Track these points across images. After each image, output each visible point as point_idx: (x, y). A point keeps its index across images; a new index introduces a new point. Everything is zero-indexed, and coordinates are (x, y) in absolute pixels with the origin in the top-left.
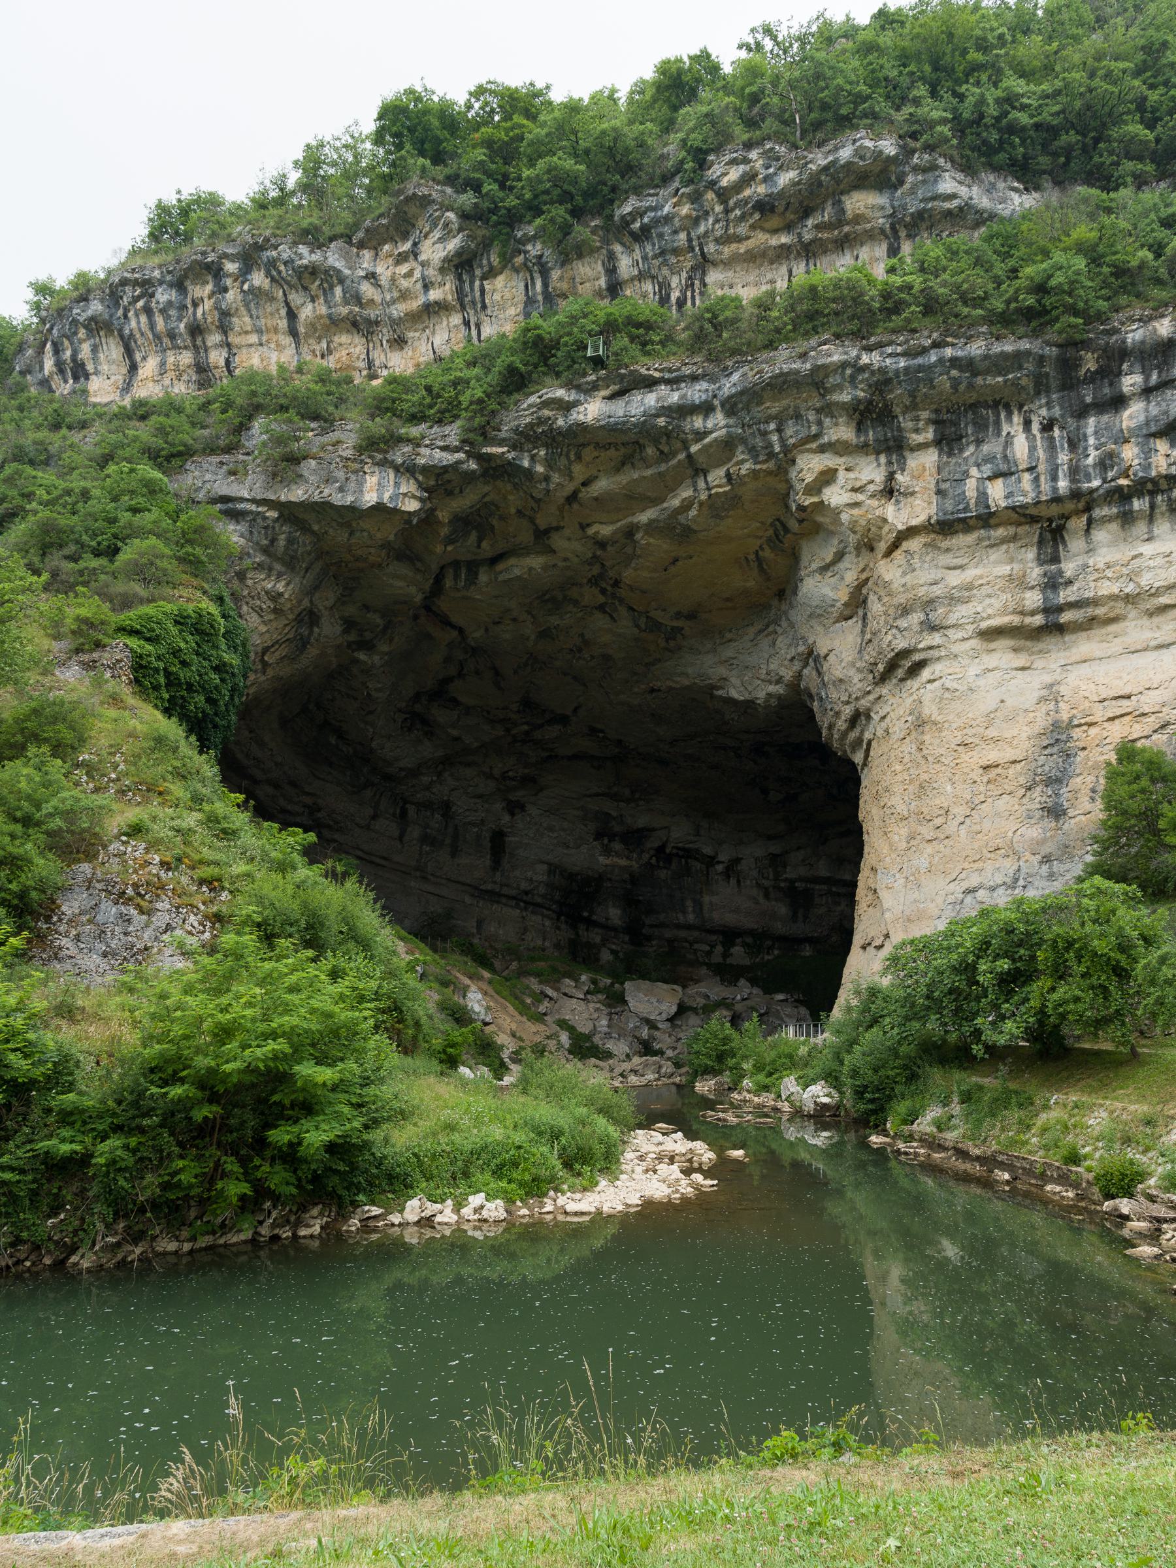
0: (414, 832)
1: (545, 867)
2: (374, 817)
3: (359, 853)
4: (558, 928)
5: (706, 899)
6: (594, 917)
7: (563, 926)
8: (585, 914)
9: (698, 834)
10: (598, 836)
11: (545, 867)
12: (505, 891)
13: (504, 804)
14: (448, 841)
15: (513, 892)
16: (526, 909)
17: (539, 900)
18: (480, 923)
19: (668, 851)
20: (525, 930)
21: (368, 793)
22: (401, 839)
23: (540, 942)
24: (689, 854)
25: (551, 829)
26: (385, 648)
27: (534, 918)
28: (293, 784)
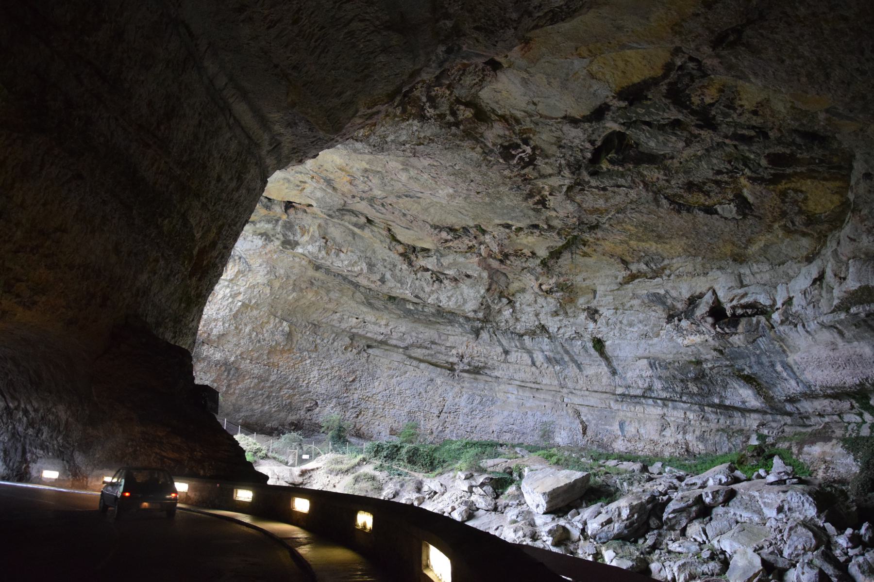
0: (539, 358)
1: (645, 361)
2: (506, 352)
3: (518, 383)
4: (707, 420)
5: (791, 359)
6: (727, 403)
7: (712, 417)
8: (717, 401)
9: (742, 285)
10: (670, 318)
11: (645, 361)
12: (633, 392)
13: (586, 313)
14: (567, 358)
15: (639, 392)
16: (665, 405)
17: (664, 395)
18: (622, 425)
19: (728, 313)
20: (663, 429)
21: (484, 335)
22: (534, 364)
23: (680, 437)
24: (756, 309)
25: (631, 325)
26: (306, 238)
27: (675, 413)
28: (433, 343)
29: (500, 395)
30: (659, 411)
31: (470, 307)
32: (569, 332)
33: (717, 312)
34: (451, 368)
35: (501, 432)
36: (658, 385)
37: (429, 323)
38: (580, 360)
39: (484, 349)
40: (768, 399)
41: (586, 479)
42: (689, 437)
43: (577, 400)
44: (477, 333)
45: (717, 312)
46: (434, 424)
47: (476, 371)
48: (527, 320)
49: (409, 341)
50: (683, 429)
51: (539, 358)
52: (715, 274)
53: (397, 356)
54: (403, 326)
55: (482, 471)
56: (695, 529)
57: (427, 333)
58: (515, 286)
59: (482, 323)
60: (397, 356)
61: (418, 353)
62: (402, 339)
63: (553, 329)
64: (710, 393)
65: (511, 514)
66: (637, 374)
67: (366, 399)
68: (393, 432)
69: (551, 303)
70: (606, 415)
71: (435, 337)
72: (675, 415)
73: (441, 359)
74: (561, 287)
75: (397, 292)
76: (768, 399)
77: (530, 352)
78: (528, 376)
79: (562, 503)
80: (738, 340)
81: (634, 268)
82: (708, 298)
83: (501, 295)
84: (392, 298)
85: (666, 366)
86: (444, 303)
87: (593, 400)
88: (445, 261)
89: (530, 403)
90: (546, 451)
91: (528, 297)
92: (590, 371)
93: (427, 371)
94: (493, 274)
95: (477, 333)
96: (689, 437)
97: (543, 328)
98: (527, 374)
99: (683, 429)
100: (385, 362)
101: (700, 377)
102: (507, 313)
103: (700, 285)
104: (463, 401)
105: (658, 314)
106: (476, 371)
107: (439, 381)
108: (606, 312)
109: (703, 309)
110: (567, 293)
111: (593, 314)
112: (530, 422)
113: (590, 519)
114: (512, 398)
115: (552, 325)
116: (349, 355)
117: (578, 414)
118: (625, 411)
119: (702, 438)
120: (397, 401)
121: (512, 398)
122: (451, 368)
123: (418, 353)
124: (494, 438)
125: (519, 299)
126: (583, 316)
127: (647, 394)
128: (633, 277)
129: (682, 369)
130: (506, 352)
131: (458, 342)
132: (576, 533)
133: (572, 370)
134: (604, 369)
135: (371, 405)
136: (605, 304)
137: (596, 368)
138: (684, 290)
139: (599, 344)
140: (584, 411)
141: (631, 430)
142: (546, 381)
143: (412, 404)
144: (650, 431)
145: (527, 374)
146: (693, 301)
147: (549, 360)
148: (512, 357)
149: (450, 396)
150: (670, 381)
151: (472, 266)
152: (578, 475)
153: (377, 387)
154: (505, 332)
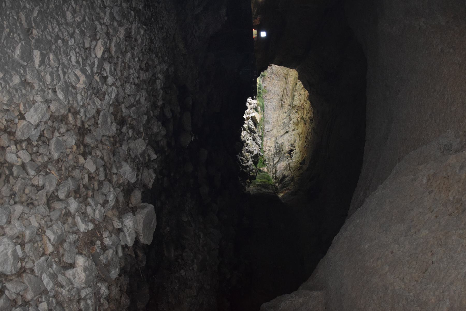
2: (286, 113)
21: (289, 107)
29: (276, 112)
30: (273, 146)
31: (295, 103)
32: (290, 126)
33: (292, 151)
34: (282, 100)
35: (267, 113)
36: (278, 145)
37: (292, 93)
38: (284, 129)
39: (286, 107)
40: (275, 164)
41: (258, 123)
42: (268, 152)
43: (275, 130)
44: (290, 105)
45: (292, 151)
46: (268, 97)
47: (282, 106)
48: (292, 116)
49: (287, 89)
50: (269, 150)
51: (284, 120)
52: (298, 149)
53: (284, 86)
54: (291, 87)
55: (258, 106)
56: (251, 138)
57: (290, 93)
58: (299, 112)
59: (292, 106)
60: (284, 86)
61: (285, 91)
62: (288, 87)
63: (291, 122)
64: (277, 154)
65: (251, 111)
66: (281, 140)
67: (273, 79)
68: (265, 87)
69: (296, 121)
70: (272, 136)
71: (289, 95)
72: (272, 149)
73: (284, 97)
74: (298, 122)
75: (297, 85)
76: (275, 164)
77: (286, 118)
78: (280, 118)
79: (254, 119)
80: (286, 155)
81: (301, 135)
82: (294, 149)
83: (297, 110)
84: (296, 84)
85: (282, 145)
86: (296, 97)
87: (275, 133)
88: (303, 96)
89: (274, 119)
90: (263, 119)
91: (297, 116)
92: (282, 132)
93: (281, 94)
94: (301, 107)
95: (290, 105)
96: (268, 152)
97: (291, 120)
98: (281, 118)
99: (269, 150)
100: (283, 83)
101: (280, 151)
102: (294, 112)
103: (297, 147)
104: (274, 104)
105: (293, 142)
106: (282, 106)
107: (279, 97)
108: (294, 132)
109: (292, 148)
110: (297, 124)
111: (294, 130)
112: (270, 120)
113: (251, 123)
114: (275, 115)
115: (291, 122)
116: (283, 74)
117: (272, 130)
118: (273, 140)
119: (267, 154)
120: (273, 87)
121: (275, 115)
122: (282, 100)
123: (285, 91)
124: (265, 111)
125: (297, 114)
126: (293, 128)
127: (277, 143)
128: (299, 136)
129: (281, 148)
130: (286, 113)
131: (288, 101)
132: (249, 121)
133: (282, 128)
134: (282, 134)
135: (271, 80)
136: (296, 131)
137: (282, 132)
138: (296, 145)
139: (287, 132)
140: (273, 131)
141: (269, 141)
142: (279, 122)
143: (272, 91)
144: (269, 144)
145: (281, 118)
146: (294, 147)
147: (284, 122)
148: (285, 114)
149: (275, 100)
150: (279, 147)
151: (302, 102)
152: (258, 121)
153: (276, 82)
154: (290, 112)
